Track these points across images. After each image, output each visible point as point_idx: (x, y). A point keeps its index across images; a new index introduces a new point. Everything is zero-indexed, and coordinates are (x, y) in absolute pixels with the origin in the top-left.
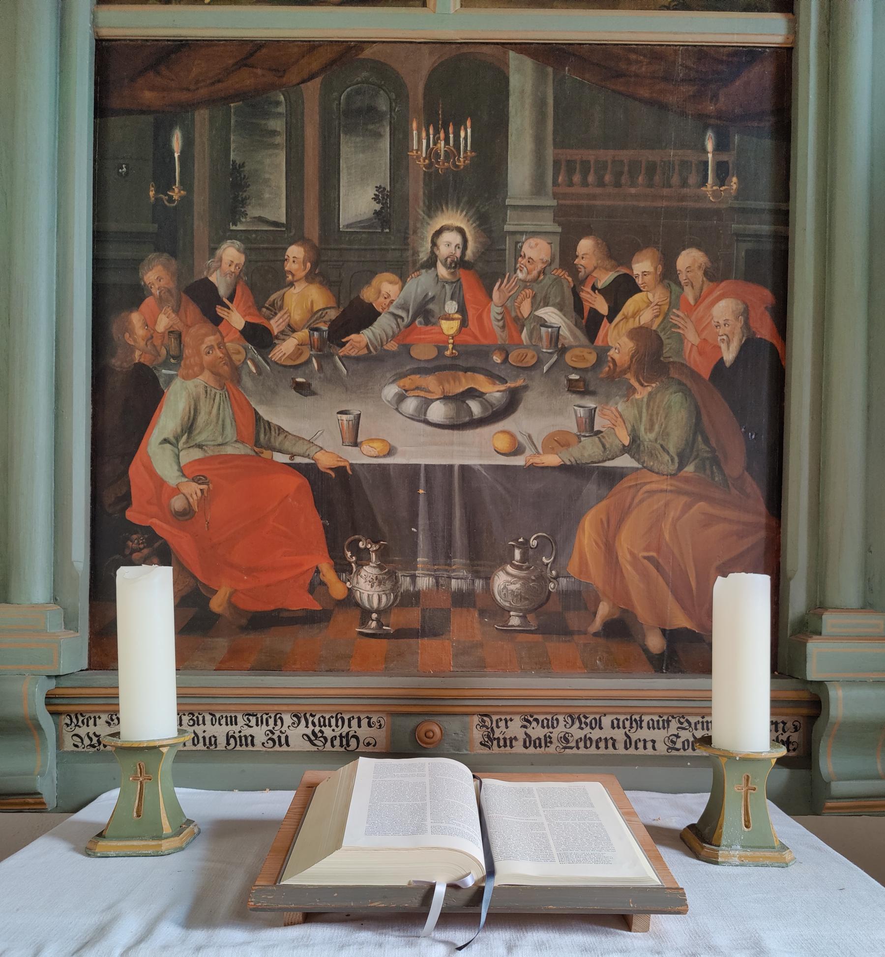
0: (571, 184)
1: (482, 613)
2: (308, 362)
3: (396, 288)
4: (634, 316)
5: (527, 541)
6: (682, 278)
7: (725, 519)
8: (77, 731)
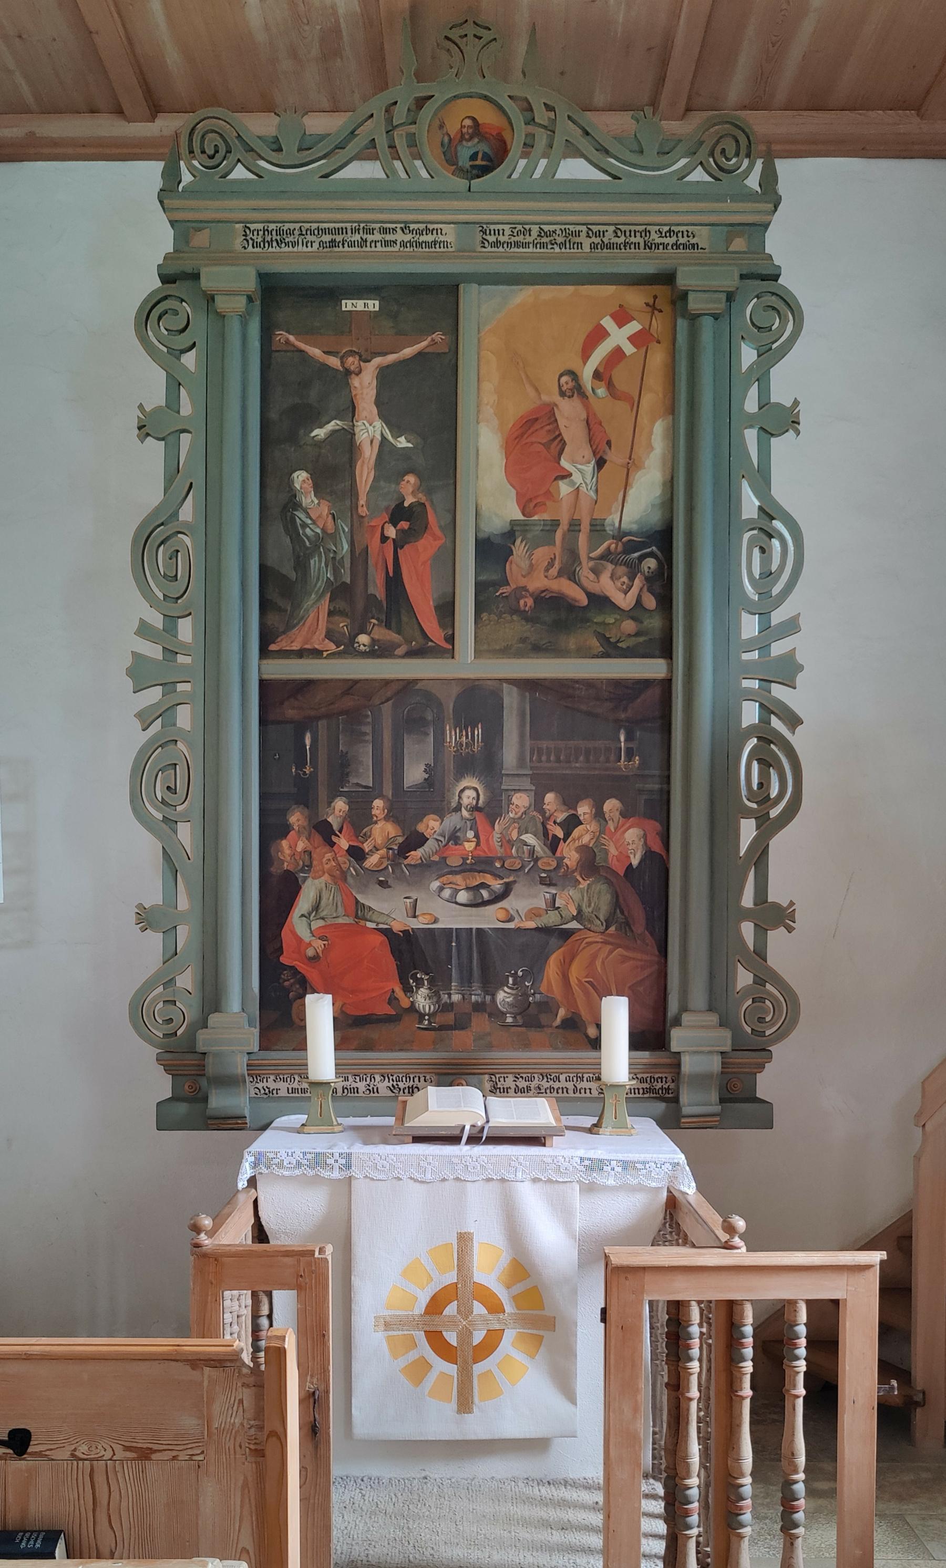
0: (540, 761)
1: (490, 1015)
2: (386, 868)
3: (438, 823)
4: (579, 839)
5: (516, 973)
6: (607, 816)
7: (634, 959)
8: (257, 1085)
